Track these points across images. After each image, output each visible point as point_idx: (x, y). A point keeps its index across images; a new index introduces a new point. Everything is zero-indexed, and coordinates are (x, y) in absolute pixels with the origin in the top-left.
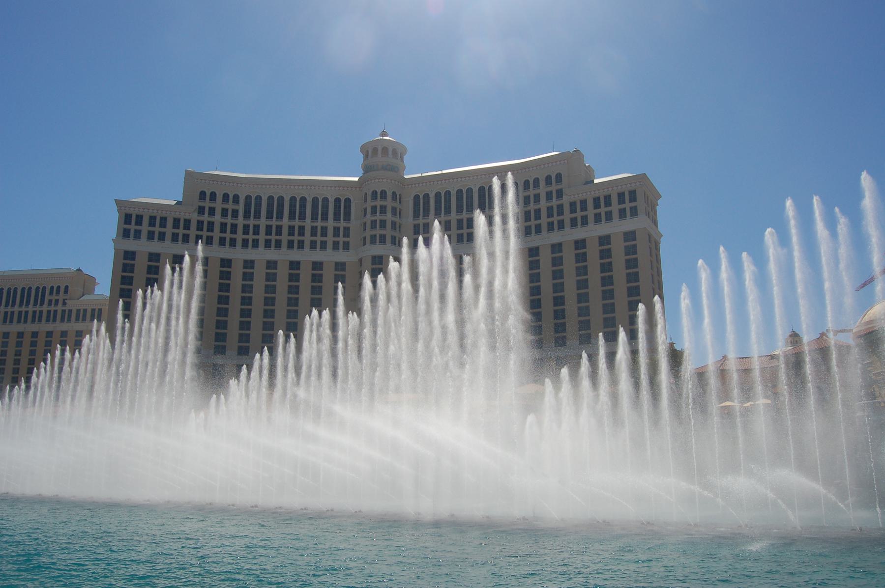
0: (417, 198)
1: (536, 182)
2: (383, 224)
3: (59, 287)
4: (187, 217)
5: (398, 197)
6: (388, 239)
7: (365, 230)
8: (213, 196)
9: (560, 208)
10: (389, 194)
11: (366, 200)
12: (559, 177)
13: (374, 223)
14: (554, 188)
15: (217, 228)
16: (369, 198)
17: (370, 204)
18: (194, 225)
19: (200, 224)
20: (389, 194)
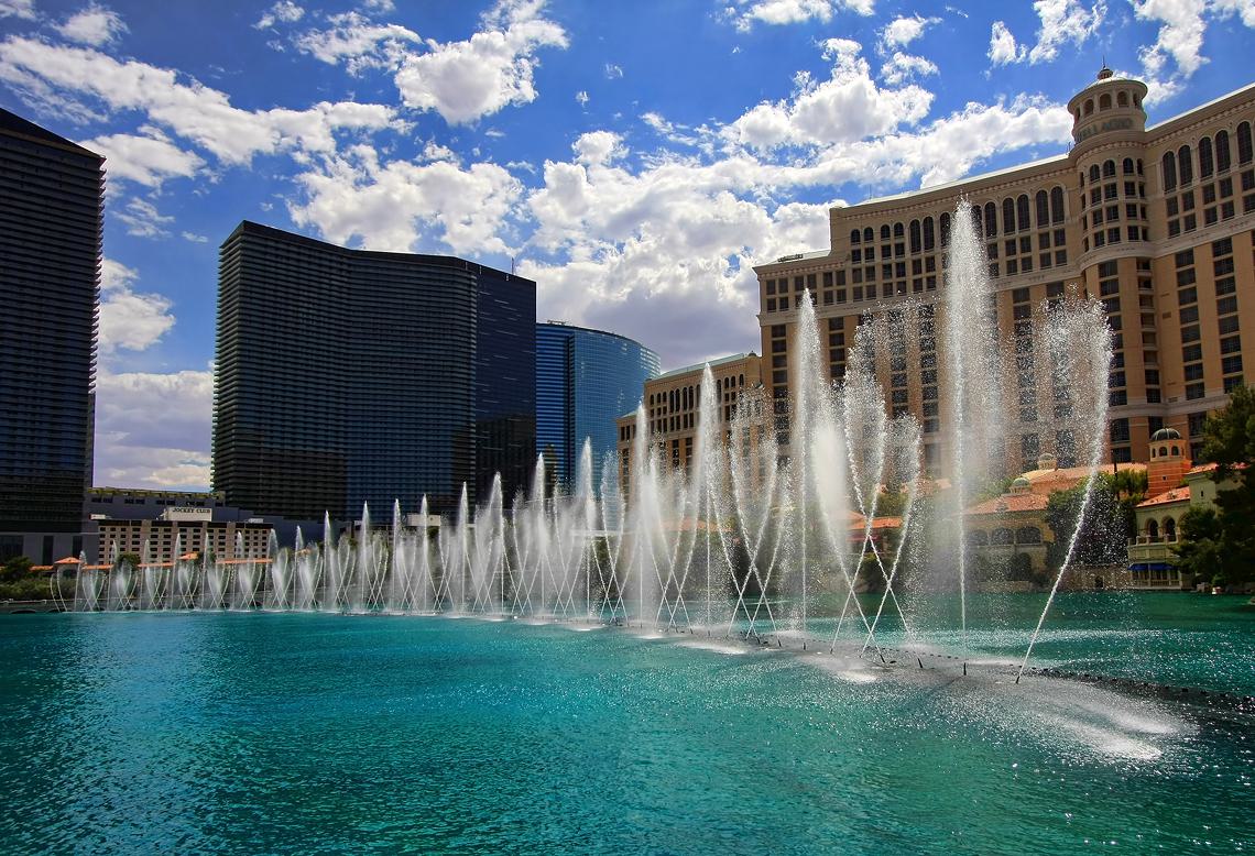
0: (1168, 157)
2: (1113, 213)
3: (733, 378)
4: (839, 267)
5: (1135, 164)
6: (1124, 234)
7: (1086, 227)
8: (869, 233)
10: (1119, 165)
11: (1082, 184)
15: (879, 272)
18: (849, 277)
20: (1119, 165)
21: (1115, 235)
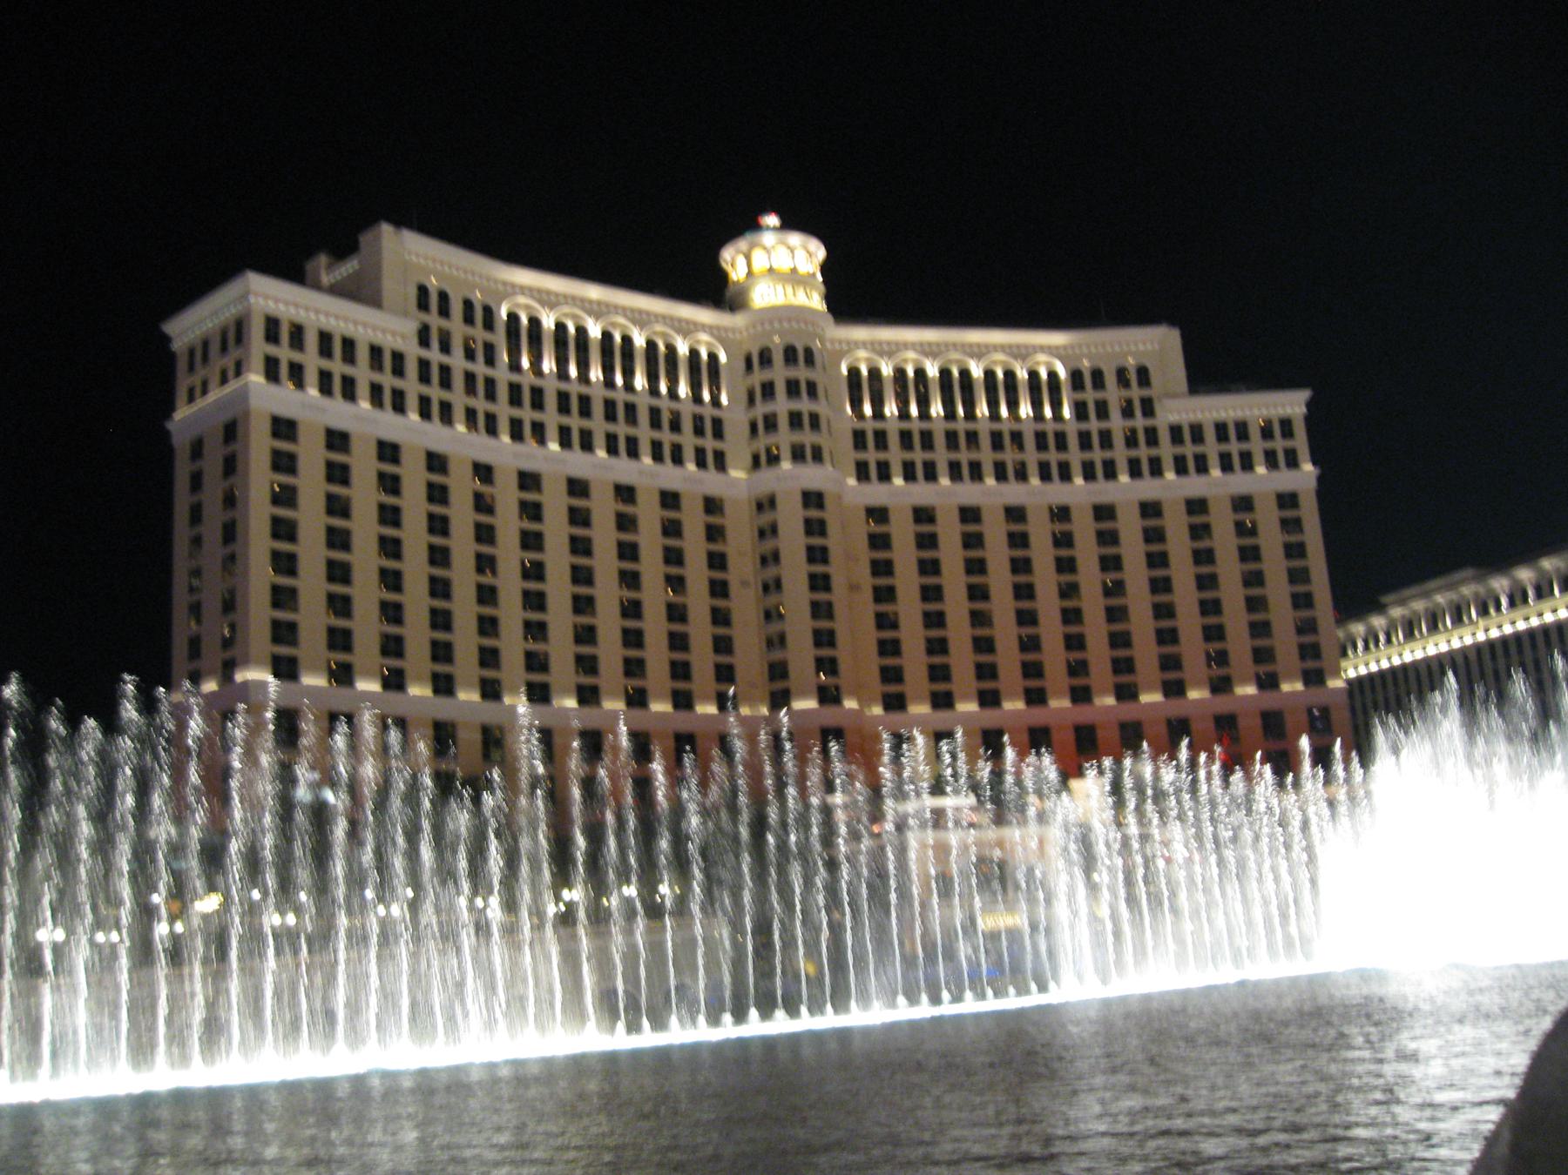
0: (854, 373)
1: (1098, 377)
4: (399, 345)
9: (1152, 437)
12: (1143, 375)
13: (795, 420)
14: (1136, 393)
16: (778, 358)
17: (779, 373)
18: (412, 368)
19: (424, 365)
21: (818, 455)
